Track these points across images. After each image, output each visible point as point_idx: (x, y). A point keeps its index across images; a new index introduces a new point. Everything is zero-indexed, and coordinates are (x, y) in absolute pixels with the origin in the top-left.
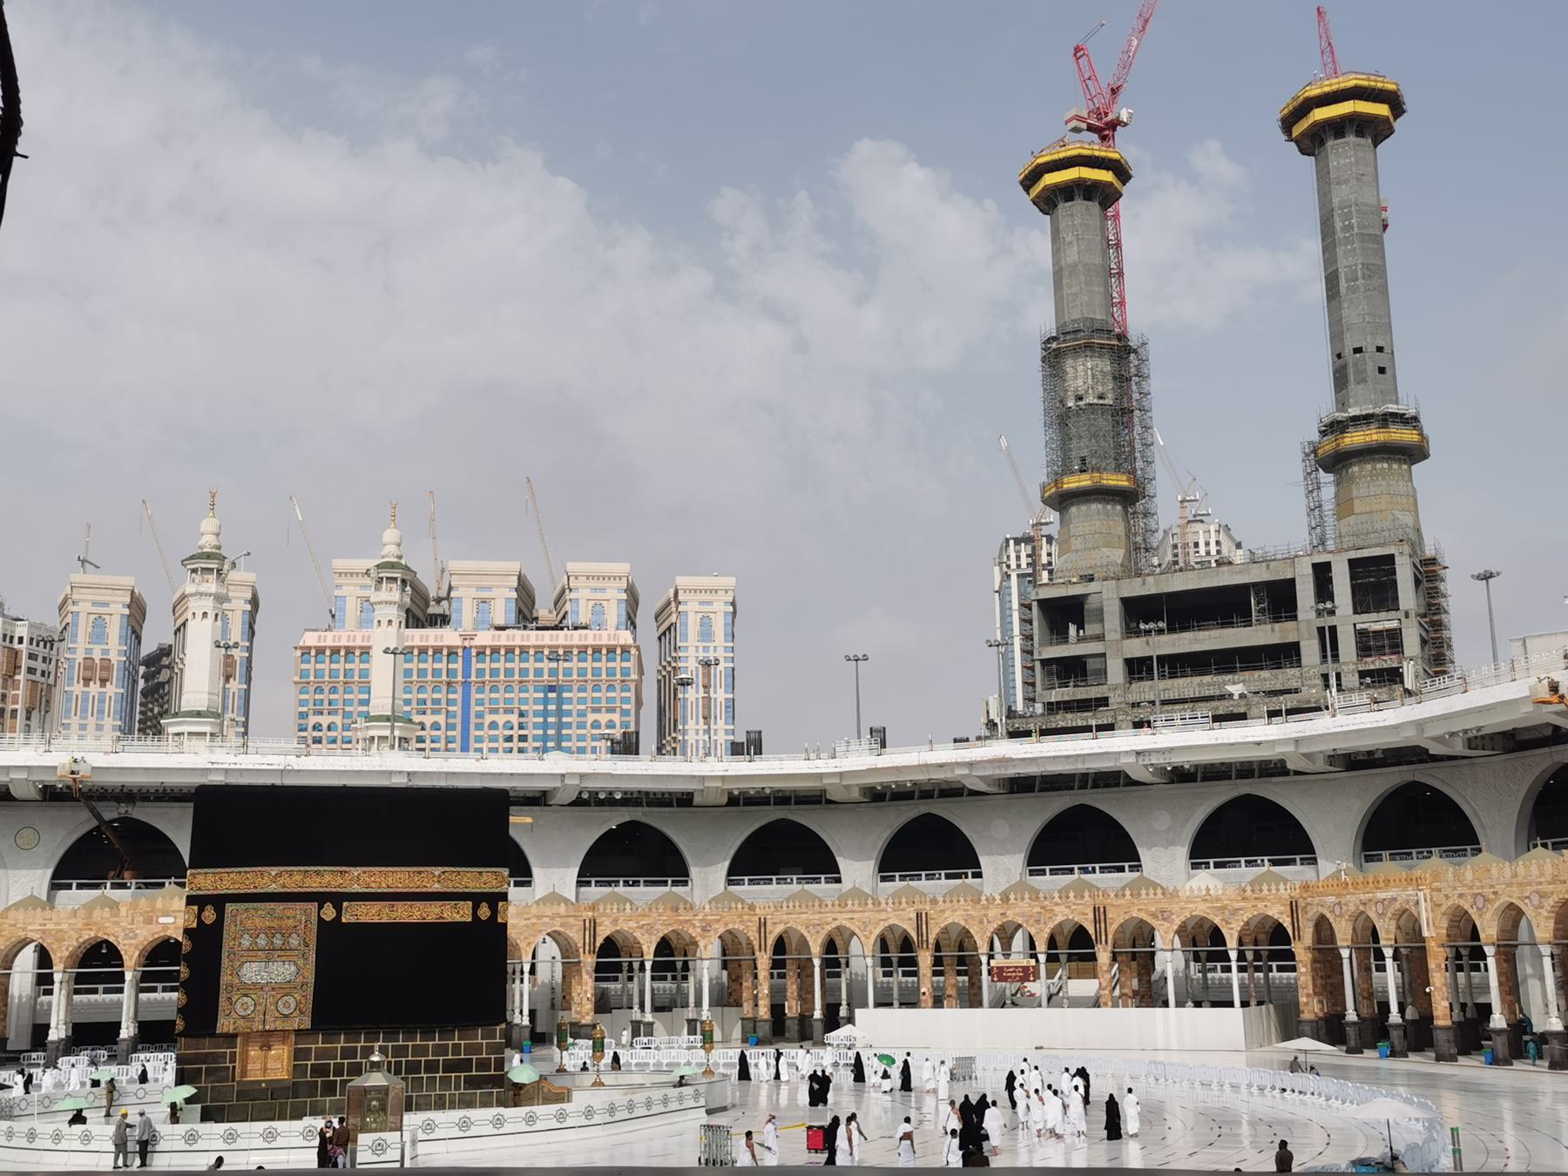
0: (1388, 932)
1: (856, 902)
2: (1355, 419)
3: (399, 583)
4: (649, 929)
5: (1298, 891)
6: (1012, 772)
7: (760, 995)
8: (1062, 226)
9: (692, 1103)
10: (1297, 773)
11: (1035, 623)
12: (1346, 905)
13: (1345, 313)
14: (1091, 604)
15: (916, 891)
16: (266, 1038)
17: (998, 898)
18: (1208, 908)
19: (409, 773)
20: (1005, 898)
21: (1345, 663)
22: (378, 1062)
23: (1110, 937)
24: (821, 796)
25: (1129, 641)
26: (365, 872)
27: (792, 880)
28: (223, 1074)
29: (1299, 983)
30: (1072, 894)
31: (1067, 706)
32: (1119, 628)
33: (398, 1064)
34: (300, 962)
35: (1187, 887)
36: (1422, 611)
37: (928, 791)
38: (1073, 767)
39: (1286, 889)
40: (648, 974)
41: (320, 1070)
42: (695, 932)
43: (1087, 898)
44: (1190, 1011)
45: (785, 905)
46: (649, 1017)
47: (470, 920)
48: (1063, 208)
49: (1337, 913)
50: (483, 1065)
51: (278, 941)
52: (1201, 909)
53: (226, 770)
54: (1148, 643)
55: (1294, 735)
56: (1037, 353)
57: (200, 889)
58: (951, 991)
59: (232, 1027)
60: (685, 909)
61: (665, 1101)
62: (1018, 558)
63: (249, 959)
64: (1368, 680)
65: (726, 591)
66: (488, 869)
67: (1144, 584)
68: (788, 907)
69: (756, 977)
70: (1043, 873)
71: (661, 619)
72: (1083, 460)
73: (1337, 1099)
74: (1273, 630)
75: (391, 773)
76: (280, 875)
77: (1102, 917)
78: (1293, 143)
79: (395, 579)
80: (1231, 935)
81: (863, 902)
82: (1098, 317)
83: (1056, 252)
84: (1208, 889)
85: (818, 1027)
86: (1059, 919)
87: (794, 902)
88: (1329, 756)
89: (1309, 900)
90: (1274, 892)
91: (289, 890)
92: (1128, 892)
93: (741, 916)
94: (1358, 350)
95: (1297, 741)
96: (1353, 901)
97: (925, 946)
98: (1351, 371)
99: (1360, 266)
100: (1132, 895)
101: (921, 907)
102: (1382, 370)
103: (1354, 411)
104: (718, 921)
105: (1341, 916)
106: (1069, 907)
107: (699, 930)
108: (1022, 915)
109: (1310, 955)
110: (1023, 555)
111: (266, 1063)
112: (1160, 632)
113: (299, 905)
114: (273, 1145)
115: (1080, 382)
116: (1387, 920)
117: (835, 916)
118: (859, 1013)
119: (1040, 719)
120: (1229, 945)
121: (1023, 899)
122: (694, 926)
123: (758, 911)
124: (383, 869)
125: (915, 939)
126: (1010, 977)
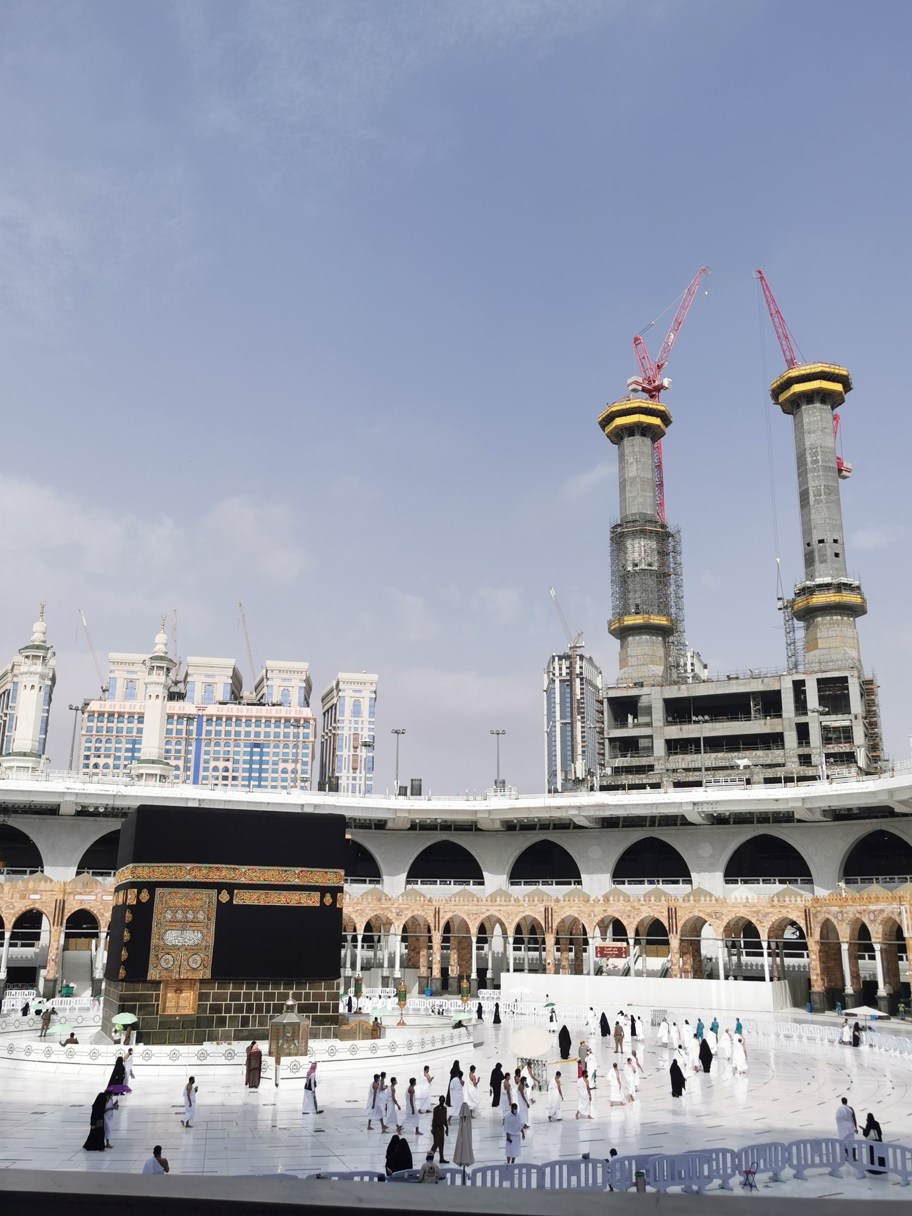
0: (877, 933)
1: (503, 899)
2: (820, 586)
3: (165, 670)
4: (361, 913)
5: (810, 902)
6: (607, 813)
7: (434, 961)
8: (627, 451)
9: (465, 1040)
10: (799, 821)
11: (606, 714)
12: (846, 913)
13: (813, 516)
14: (643, 702)
15: (543, 893)
16: (179, 985)
17: (602, 899)
18: (747, 911)
19: (199, 800)
20: (606, 899)
21: (814, 748)
22: (292, 1006)
23: (679, 929)
24: (472, 826)
25: (668, 727)
26: (249, 870)
27: (450, 882)
28: (150, 1009)
29: (811, 966)
30: (653, 899)
31: (629, 770)
32: (662, 719)
33: (268, 1005)
34: (205, 931)
35: (733, 897)
36: (864, 715)
37: (545, 825)
38: (649, 812)
39: (802, 901)
40: (359, 944)
41: (216, 1009)
42: (392, 916)
43: (663, 901)
44: (731, 981)
45: (453, 899)
46: (359, 973)
47: (319, 905)
48: (627, 441)
49: (840, 917)
50: (325, 1008)
51: (179, 916)
52: (743, 912)
53: (77, 794)
54: (681, 730)
55: (803, 796)
56: (608, 535)
57: (139, 877)
58: (564, 963)
59: (158, 976)
60: (386, 899)
61: (452, 1038)
62: (560, 669)
63: (171, 928)
64: (832, 760)
65: (371, 684)
66: (331, 870)
67: (679, 689)
68: (455, 901)
69: (430, 948)
70: (623, 883)
71: (326, 701)
72: (637, 606)
73: (895, 1050)
74: (765, 724)
75: (187, 799)
76: (192, 869)
77: (674, 915)
78: (779, 407)
79: (163, 668)
80: (763, 930)
81: (508, 899)
82: (649, 512)
83: (622, 469)
84: (747, 899)
85: (474, 985)
86: (644, 915)
87: (459, 897)
88: (824, 811)
89: (819, 909)
90: (793, 902)
91: (198, 880)
92: (692, 898)
93: (423, 906)
94: (821, 541)
95: (804, 800)
96: (852, 911)
97: (550, 931)
98: (816, 554)
99: (822, 487)
100: (694, 900)
101: (548, 904)
102: (837, 555)
103: (819, 581)
104: (407, 909)
105: (842, 920)
106: (649, 907)
107: (394, 915)
108: (618, 911)
109: (818, 947)
110: (564, 667)
111: (178, 1002)
112: (706, 722)
113: (205, 891)
114: (204, 1062)
115: (636, 555)
116: (877, 925)
117: (488, 908)
118: (503, 975)
119: (610, 778)
120: (762, 938)
121: (619, 900)
122: (391, 912)
123: (434, 903)
124: (262, 867)
125: (543, 926)
126: (609, 954)
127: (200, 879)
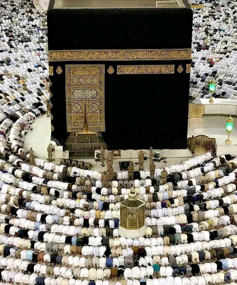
47: (174, 73)
127: (94, 59)
